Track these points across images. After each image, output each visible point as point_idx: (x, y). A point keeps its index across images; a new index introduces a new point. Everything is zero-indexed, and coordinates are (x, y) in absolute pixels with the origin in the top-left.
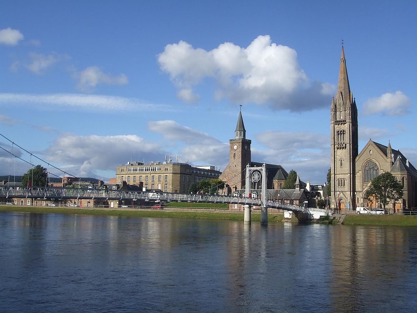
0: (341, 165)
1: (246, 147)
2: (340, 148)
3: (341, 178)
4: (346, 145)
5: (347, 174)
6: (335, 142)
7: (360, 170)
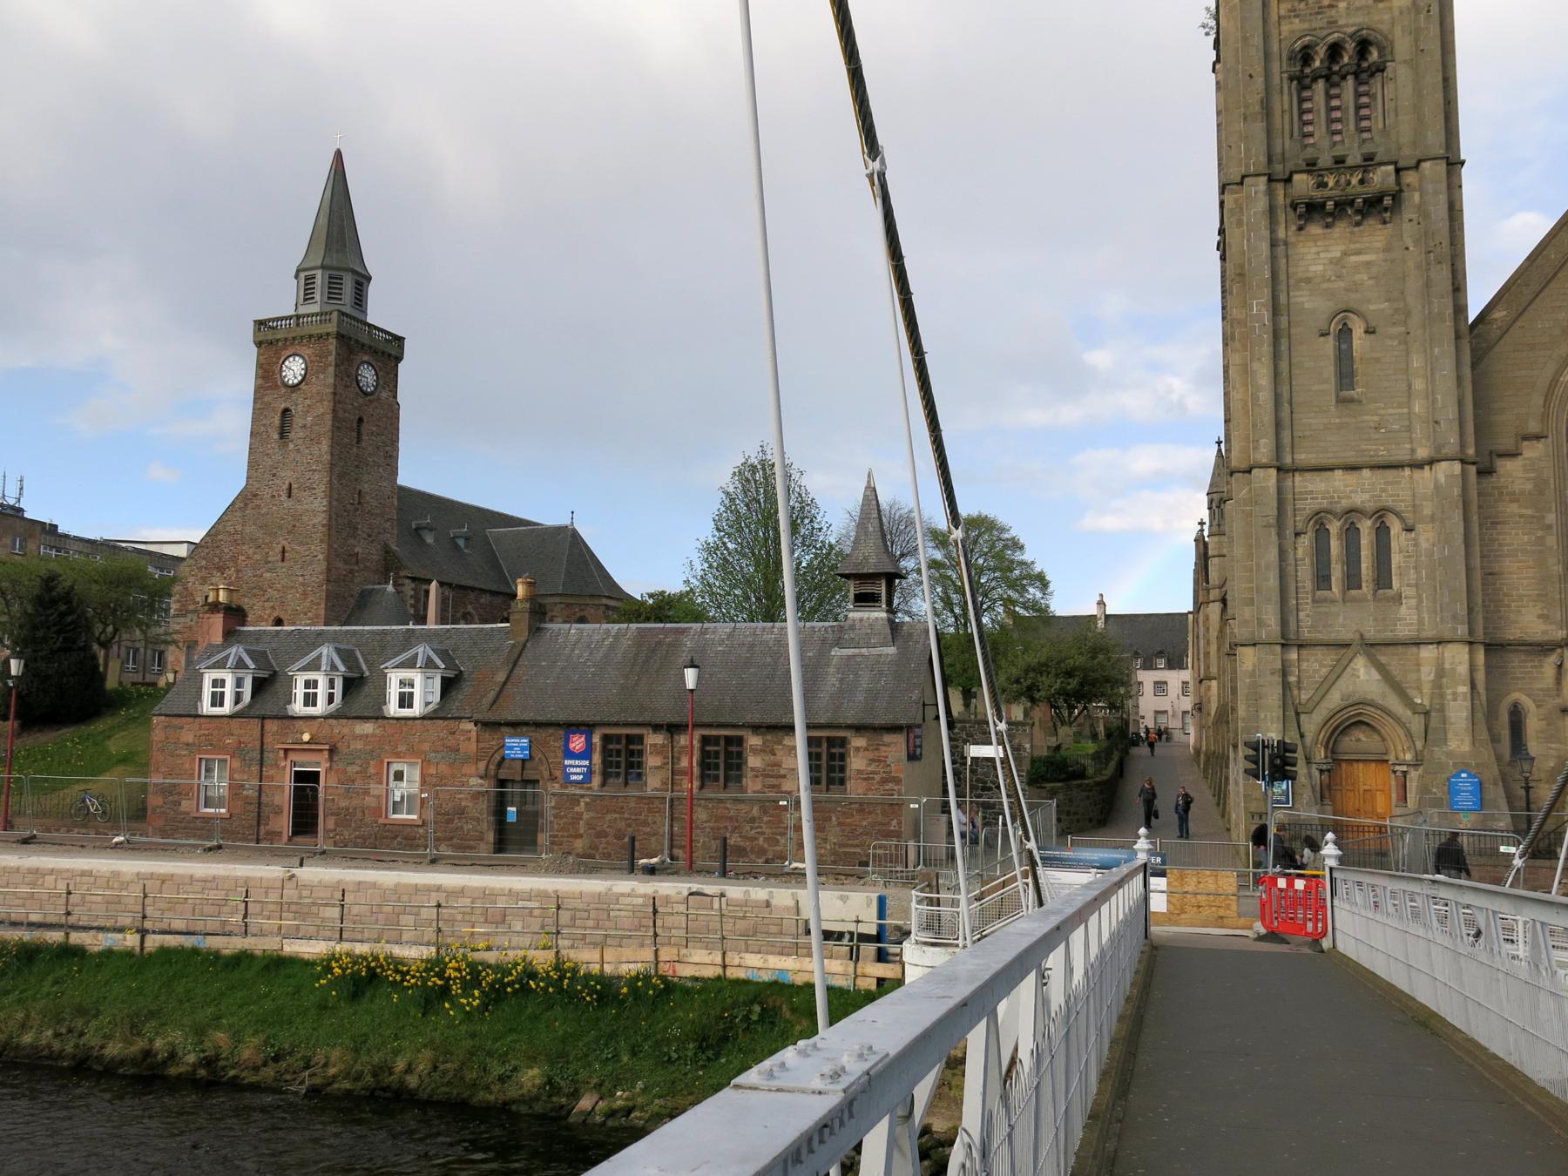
0: (1345, 372)
1: (368, 376)
2: (1343, 206)
3: (1345, 504)
4: (1398, 171)
5: (1418, 465)
6: (1278, 150)
7: (1533, 427)
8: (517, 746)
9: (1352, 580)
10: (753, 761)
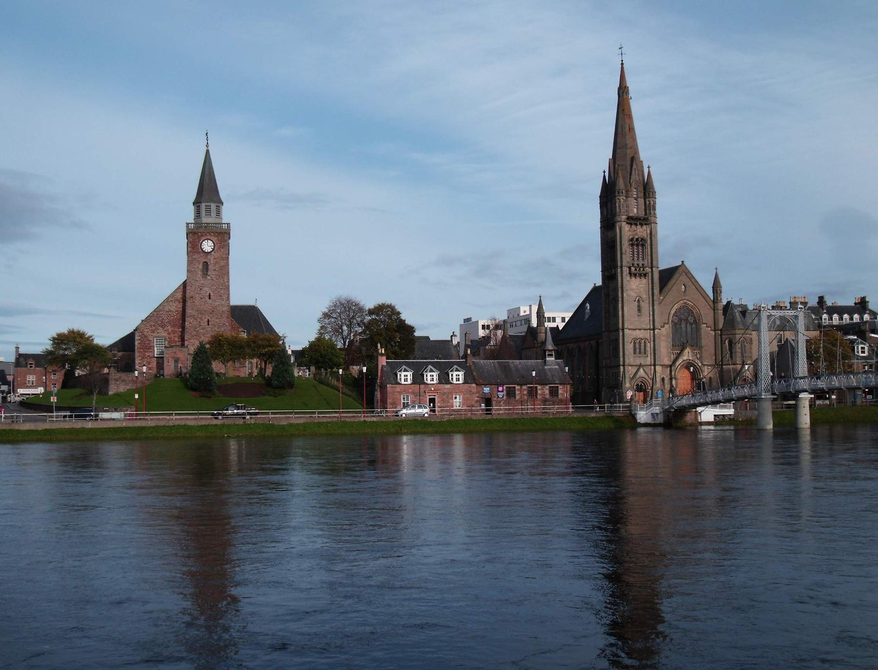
8: (487, 390)
9: (640, 353)
10: (539, 392)
